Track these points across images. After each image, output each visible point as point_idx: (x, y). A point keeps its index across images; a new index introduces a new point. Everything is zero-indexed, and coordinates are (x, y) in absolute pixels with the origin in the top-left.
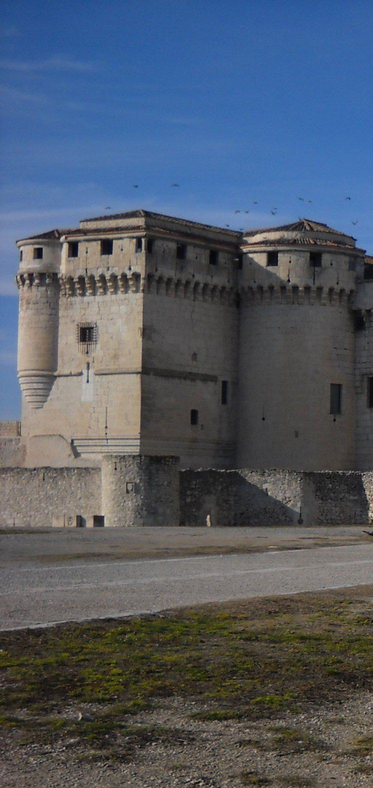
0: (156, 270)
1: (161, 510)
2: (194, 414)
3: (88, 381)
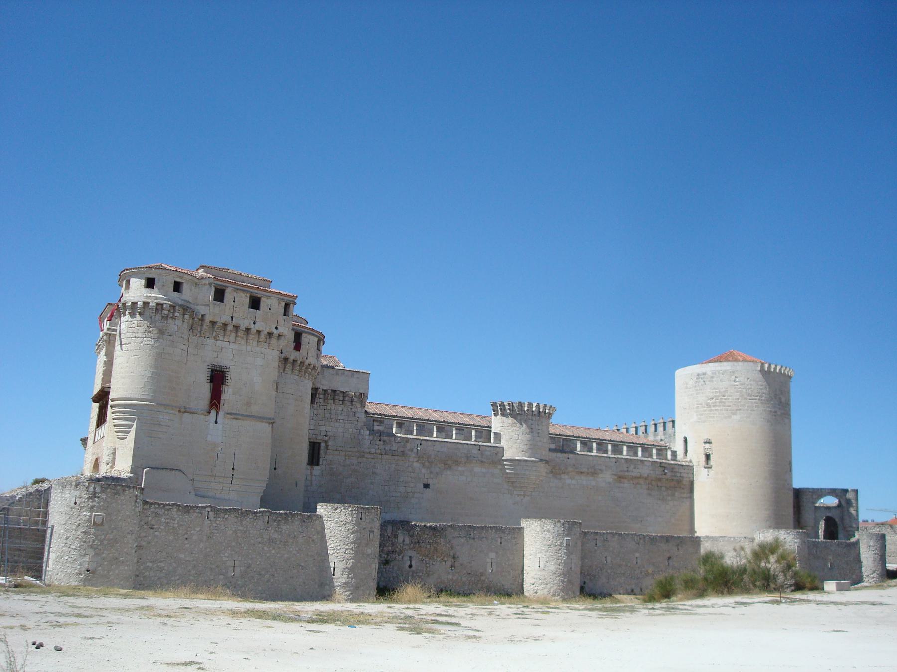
3: (216, 422)
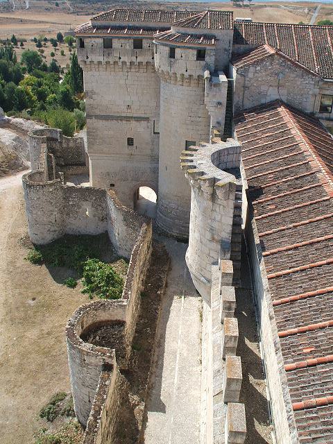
0: (88, 58)
1: (34, 212)
2: (130, 142)
